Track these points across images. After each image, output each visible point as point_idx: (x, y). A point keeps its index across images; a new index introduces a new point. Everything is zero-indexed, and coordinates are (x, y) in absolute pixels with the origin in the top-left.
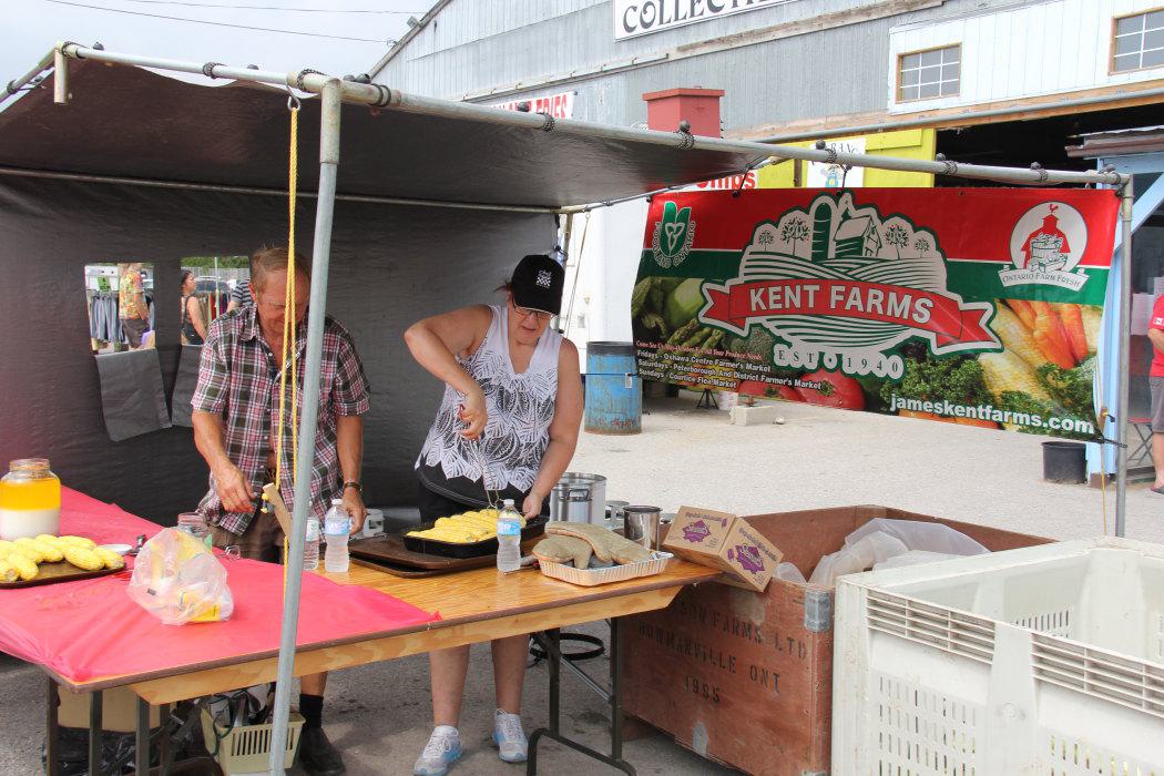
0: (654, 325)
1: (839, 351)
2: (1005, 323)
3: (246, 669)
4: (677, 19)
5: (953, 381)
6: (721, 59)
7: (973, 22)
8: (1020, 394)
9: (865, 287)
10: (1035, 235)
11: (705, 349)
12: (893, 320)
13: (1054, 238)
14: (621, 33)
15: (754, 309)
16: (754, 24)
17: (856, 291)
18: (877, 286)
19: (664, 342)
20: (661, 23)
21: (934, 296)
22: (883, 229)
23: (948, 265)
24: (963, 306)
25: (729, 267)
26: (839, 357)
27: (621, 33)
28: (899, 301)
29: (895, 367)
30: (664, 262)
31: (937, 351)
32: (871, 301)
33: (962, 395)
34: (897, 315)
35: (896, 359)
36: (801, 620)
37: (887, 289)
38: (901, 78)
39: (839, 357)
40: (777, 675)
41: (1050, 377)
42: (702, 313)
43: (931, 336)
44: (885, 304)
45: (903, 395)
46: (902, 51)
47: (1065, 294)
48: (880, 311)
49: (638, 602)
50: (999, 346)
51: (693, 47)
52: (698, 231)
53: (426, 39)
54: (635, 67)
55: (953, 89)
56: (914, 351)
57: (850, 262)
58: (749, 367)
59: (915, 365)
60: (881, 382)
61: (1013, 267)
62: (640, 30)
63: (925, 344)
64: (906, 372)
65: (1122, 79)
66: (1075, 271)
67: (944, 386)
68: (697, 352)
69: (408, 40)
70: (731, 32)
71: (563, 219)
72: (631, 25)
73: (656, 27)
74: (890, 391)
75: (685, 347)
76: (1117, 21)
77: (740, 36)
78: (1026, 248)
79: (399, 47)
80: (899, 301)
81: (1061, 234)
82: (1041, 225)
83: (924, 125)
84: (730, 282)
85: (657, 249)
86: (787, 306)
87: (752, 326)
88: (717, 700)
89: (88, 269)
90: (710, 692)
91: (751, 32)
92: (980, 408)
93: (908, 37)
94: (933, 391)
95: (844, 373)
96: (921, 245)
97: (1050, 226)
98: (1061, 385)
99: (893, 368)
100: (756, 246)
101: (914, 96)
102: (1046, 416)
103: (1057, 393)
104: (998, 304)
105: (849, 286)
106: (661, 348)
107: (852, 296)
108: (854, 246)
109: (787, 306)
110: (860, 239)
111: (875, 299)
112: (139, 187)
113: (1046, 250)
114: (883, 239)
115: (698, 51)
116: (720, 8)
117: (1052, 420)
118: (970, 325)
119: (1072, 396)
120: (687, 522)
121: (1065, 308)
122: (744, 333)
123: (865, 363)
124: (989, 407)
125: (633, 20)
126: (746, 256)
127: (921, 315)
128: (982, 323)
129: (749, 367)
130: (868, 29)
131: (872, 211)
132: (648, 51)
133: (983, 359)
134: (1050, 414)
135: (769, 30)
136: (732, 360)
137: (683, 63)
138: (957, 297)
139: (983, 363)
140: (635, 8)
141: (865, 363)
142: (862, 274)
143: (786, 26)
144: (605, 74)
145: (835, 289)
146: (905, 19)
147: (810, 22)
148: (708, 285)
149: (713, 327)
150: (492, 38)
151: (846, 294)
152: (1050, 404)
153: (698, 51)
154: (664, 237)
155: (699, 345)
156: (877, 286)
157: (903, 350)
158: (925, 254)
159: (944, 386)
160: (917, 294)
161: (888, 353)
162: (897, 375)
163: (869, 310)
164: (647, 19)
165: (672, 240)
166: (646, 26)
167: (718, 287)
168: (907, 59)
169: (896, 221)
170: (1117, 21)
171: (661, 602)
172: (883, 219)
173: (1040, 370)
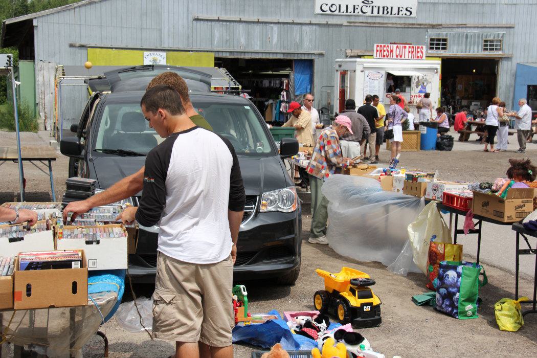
6: (364, 28)
14: (318, 11)
16: (378, 20)
20: (340, 11)
54: (327, 25)
62: (329, 12)
70: (370, 21)
73: (337, 12)
83: (439, 57)
125: (324, 8)
135: (386, 23)
143: (393, 24)
147: (401, 24)
164: (333, 9)
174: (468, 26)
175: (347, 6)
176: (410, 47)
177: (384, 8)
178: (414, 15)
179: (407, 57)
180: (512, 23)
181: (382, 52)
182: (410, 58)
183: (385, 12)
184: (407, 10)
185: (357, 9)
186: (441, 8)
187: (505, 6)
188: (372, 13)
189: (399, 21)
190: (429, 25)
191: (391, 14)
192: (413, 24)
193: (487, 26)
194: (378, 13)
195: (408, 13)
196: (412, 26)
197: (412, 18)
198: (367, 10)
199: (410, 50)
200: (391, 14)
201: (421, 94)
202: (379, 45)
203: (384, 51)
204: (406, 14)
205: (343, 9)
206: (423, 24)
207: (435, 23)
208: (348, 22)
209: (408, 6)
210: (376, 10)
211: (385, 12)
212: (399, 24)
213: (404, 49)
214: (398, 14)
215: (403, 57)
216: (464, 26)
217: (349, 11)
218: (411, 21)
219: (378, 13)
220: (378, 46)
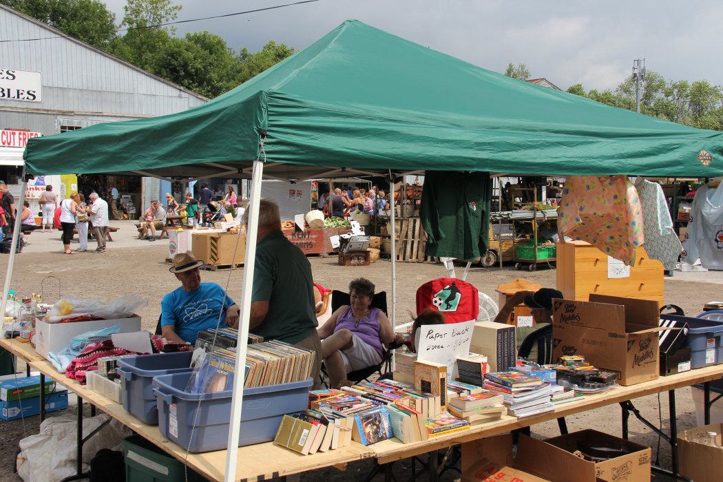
143: (10, 107)
147: (23, 109)
176: (20, 134)
179: (17, 145)
182: (17, 145)
184: (28, 93)
186: (71, 94)
187: (143, 96)
189: (19, 105)
191: (9, 96)
193: (126, 115)
195: (31, 97)
196: (37, 112)
199: (21, 136)
201: (38, 187)
204: (28, 98)
207: (65, 110)
209: (31, 89)
212: (20, 108)
213: (12, 136)
214: (18, 97)
215: (12, 145)
218: (35, 106)
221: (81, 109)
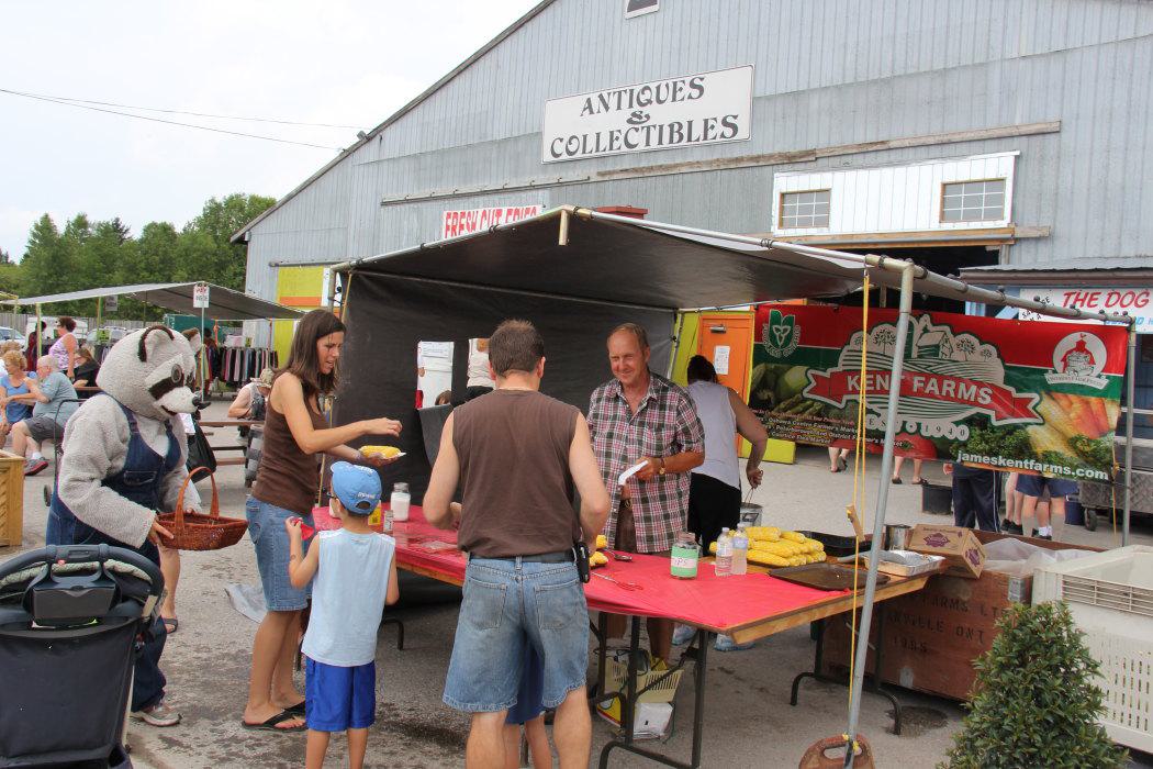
0: (766, 397)
1: (919, 420)
2: (1048, 407)
3: (772, 624)
4: (597, 150)
5: (1007, 443)
7: (839, 175)
8: (1056, 453)
9: (941, 378)
10: (1070, 352)
11: (806, 415)
12: (962, 401)
13: (1083, 355)
14: (548, 157)
15: (850, 389)
16: (662, 160)
17: (934, 381)
18: (951, 378)
19: (773, 409)
20: (584, 152)
21: (992, 386)
22: (954, 341)
23: (1005, 367)
24: (1015, 395)
25: (832, 360)
26: (919, 425)
27: (548, 157)
28: (967, 388)
29: (962, 433)
30: (775, 353)
31: (995, 423)
32: (945, 388)
33: (1013, 453)
34: (966, 398)
35: (964, 427)
36: (1006, 596)
37: (959, 380)
38: (782, 209)
39: (919, 425)
40: (981, 632)
41: (1079, 444)
42: (806, 390)
43: (992, 414)
44: (956, 391)
45: (967, 452)
46: (784, 191)
47: (1093, 391)
48: (953, 395)
49: (912, 585)
50: (1041, 421)
51: (610, 173)
52: (802, 332)
53: (370, 152)
54: (560, 184)
55: (825, 222)
56: (977, 422)
57: (931, 361)
58: (843, 429)
59: (978, 432)
60: (951, 442)
61: (1055, 372)
62: (565, 157)
63: (987, 418)
64: (971, 436)
65: (948, 226)
66: (1099, 376)
67: (999, 447)
68: (799, 417)
69: (355, 148)
70: (643, 164)
71: (679, 316)
72: (557, 151)
73: (579, 155)
74: (958, 449)
75: (789, 414)
76: (944, 185)
77: (652, 168)
78: (1064, 359)
79: (347, 154)
80: (967, 388)
81: (1088, 352)
82: (1074, 346)
84: (830, 370)
85: (767, 343)
86: (878, 388)
87: (848, 401)
88: (924, 651)
89: (422, 345)
90: (918, 646)
91: (661, 166)
92: (1026, 462)
93: (785, 181)
94: (991, 449)
95: (922, 436)
96: (987, 354)
97: (1081, 347)
98: (1087, 449)
99: (962, 433)
100: (851, 346)
101: (792, 225)
102: (1074, 468)
103: (1082, 454)
104: (1044, 395)
105: (928, 377)
106: (768, 413)
107: (930, 384)
108: (934, 350)
109: (878, 388)
110: (937, 346)
111: (949, 387)
112: (452, 287)
113: (1079, 362)
114: (955, 347)
115: (615, 177)
116: (636, 146)
117: (1078, 471)
118: (1021, 407)
119: (1094, 457)
120: (927, 534)
121: (1093, 400)
122: (842, 406)
123: (939, 429)
124: (1032, 462)
125: (559, 148)
126: (844, 352)
127: (984, 399)
128: (1030, 407)
129: (843, 429)
130: (756, 170)
131: (947, 329)
132: (571, 173)
133: (1030, 429)
134: (1077, 467)
135: (676, 166)
136: (829, 424)
137: (602, 184)
138: (1012, 389)
139: (1030, 432)
140: (561, 140)
141: (939, 429)
142: (941, 370)
143: (690, 164)
144: (533, 187)
145: (916, 379)
146: (786, 167)
147: (710, 163)
148: (814, 372)
149: (815, 400)
150: (433, 152)
151: (926, 383)
152: (1077, 460)
153: (615, 177)
154: (772, 337)
155: (802, 412)
156: (951, 378)
157: (969, 421)
158: (971, 357)
159: (999, 447)
160: (980, 385)
161: (957, 423)
162: (963, 438)
163: (944, 394)
164: (572, 148)
165: (780, 338)
166: (570, 153)
167: (821, 373)
168: (787, 197)
169: (965, 336)
170: (944, 185)
171: (919, 585)
172: (955, 333)
173: (1072, 439)
174: (892, 145)
175: (598, 135)
177: (671, 126)
178: (743, 133)
180: (1053, 116)
181: (457, 230)
183: (676, 137)
184: (725, 123)
185: (617, 138)
186: (814, 102)
187: (1022, 63)
188: (648, 144)
190: (780, 155)
191: (689, 140)
192: (738, 160)
193: (957, 138)
194: (660, 142)
195: (728, 132)
197: (740, 141)
198: (637, 138)
200: (689, 140)
202: (452, 212)
203: (462, 227)
205: (591, 144)
206: (763, 156)
208: (599, 174)
210: (654, 134)
211: (676, 137)
216: (879, 147)
217: (601, 148)
219: (660, 142)
220: (449, 216)
221: (834, 143)
